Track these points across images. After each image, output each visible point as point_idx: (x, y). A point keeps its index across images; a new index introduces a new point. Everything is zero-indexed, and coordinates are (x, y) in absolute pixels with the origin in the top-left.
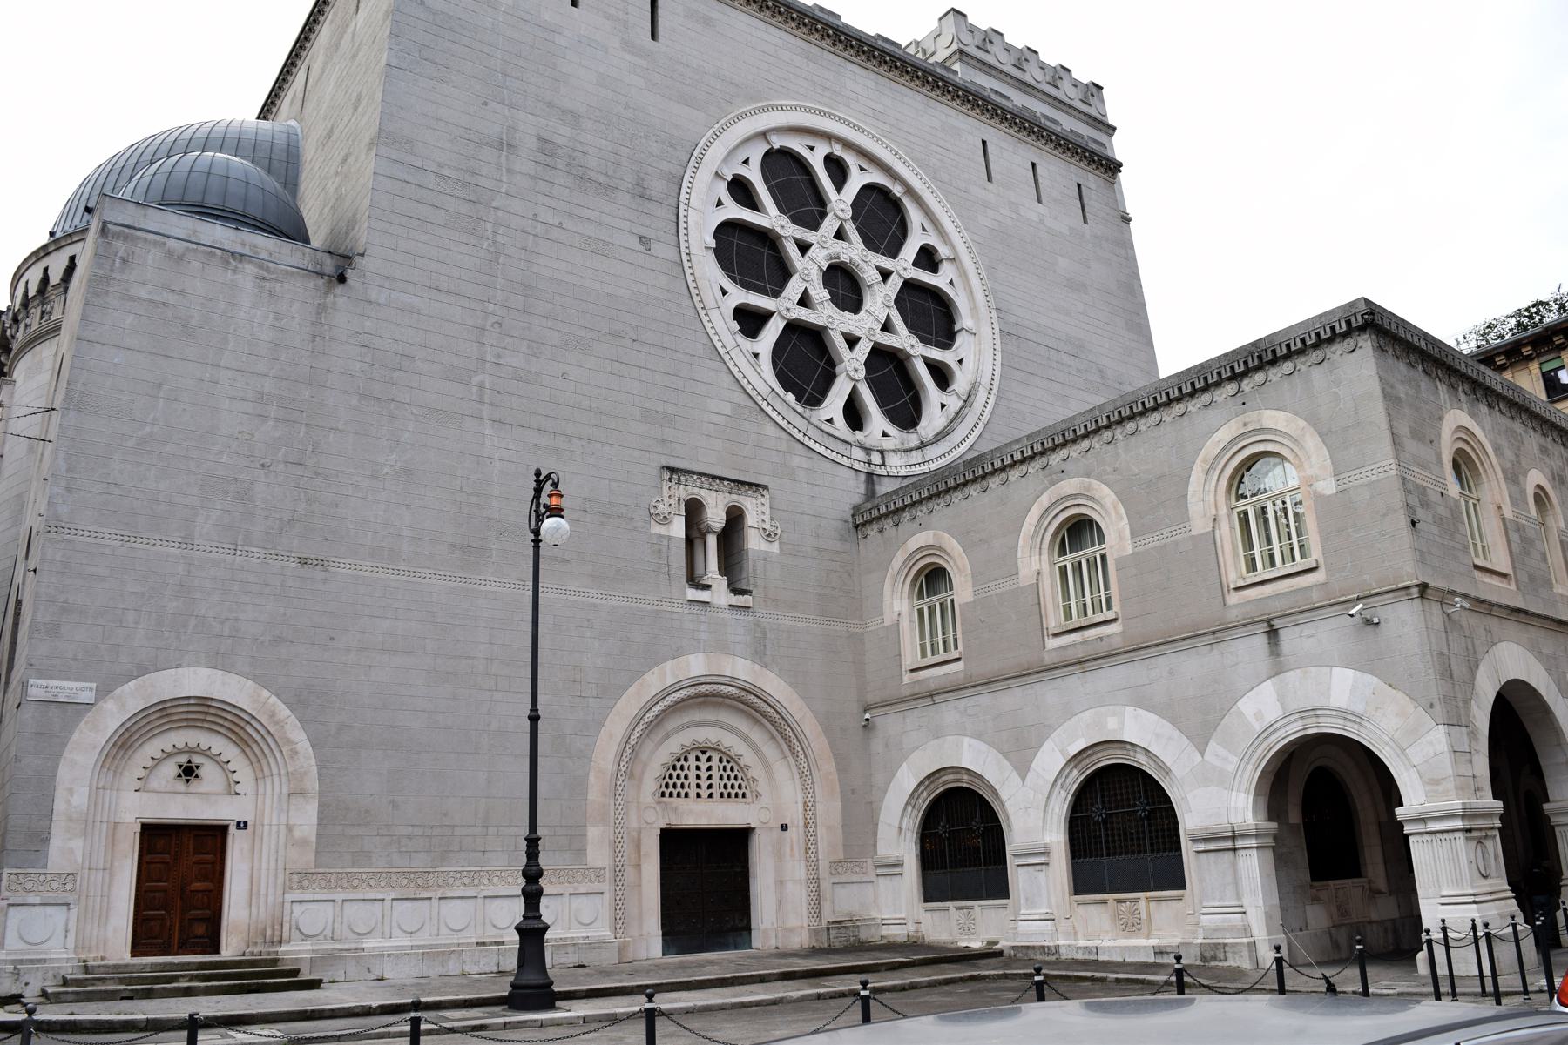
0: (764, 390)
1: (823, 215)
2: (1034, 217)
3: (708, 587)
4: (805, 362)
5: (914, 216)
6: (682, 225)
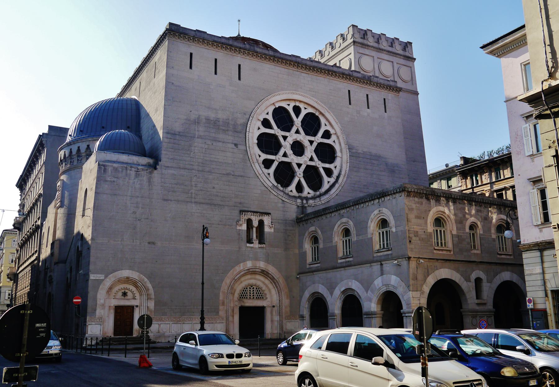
1: (292, 125)
2: (366, 114)
3: (253, 243)
4: (284, 174)
6: (247, 138)
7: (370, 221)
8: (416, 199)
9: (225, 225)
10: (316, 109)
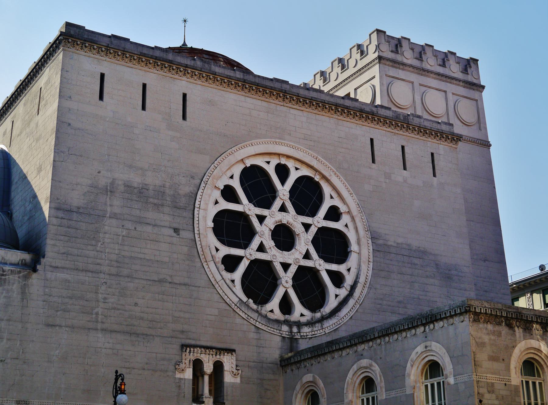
0: (236, 300)
1: (274, 198)
2: (400, 179)
4: (260, 282)
5: (327, 190)
6: (196, 219)
7: (409, 365)
8: (490, 327)
9: (155, 371)
10: (316, 170)
